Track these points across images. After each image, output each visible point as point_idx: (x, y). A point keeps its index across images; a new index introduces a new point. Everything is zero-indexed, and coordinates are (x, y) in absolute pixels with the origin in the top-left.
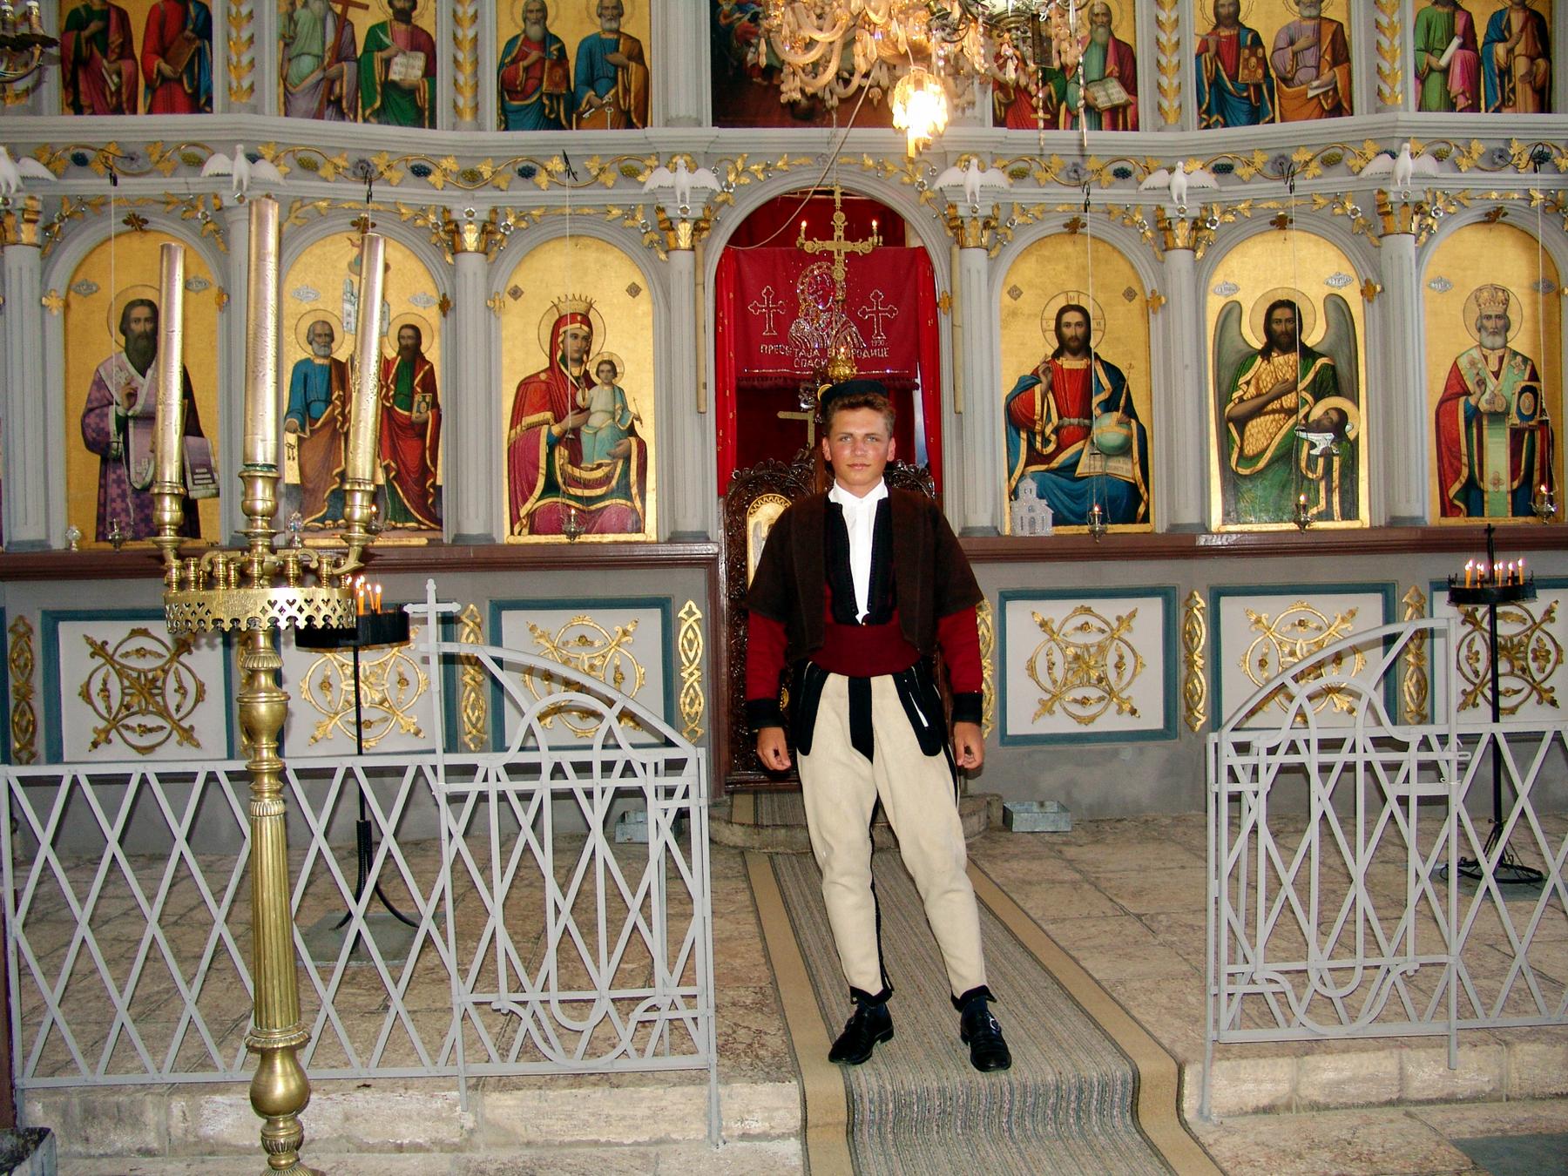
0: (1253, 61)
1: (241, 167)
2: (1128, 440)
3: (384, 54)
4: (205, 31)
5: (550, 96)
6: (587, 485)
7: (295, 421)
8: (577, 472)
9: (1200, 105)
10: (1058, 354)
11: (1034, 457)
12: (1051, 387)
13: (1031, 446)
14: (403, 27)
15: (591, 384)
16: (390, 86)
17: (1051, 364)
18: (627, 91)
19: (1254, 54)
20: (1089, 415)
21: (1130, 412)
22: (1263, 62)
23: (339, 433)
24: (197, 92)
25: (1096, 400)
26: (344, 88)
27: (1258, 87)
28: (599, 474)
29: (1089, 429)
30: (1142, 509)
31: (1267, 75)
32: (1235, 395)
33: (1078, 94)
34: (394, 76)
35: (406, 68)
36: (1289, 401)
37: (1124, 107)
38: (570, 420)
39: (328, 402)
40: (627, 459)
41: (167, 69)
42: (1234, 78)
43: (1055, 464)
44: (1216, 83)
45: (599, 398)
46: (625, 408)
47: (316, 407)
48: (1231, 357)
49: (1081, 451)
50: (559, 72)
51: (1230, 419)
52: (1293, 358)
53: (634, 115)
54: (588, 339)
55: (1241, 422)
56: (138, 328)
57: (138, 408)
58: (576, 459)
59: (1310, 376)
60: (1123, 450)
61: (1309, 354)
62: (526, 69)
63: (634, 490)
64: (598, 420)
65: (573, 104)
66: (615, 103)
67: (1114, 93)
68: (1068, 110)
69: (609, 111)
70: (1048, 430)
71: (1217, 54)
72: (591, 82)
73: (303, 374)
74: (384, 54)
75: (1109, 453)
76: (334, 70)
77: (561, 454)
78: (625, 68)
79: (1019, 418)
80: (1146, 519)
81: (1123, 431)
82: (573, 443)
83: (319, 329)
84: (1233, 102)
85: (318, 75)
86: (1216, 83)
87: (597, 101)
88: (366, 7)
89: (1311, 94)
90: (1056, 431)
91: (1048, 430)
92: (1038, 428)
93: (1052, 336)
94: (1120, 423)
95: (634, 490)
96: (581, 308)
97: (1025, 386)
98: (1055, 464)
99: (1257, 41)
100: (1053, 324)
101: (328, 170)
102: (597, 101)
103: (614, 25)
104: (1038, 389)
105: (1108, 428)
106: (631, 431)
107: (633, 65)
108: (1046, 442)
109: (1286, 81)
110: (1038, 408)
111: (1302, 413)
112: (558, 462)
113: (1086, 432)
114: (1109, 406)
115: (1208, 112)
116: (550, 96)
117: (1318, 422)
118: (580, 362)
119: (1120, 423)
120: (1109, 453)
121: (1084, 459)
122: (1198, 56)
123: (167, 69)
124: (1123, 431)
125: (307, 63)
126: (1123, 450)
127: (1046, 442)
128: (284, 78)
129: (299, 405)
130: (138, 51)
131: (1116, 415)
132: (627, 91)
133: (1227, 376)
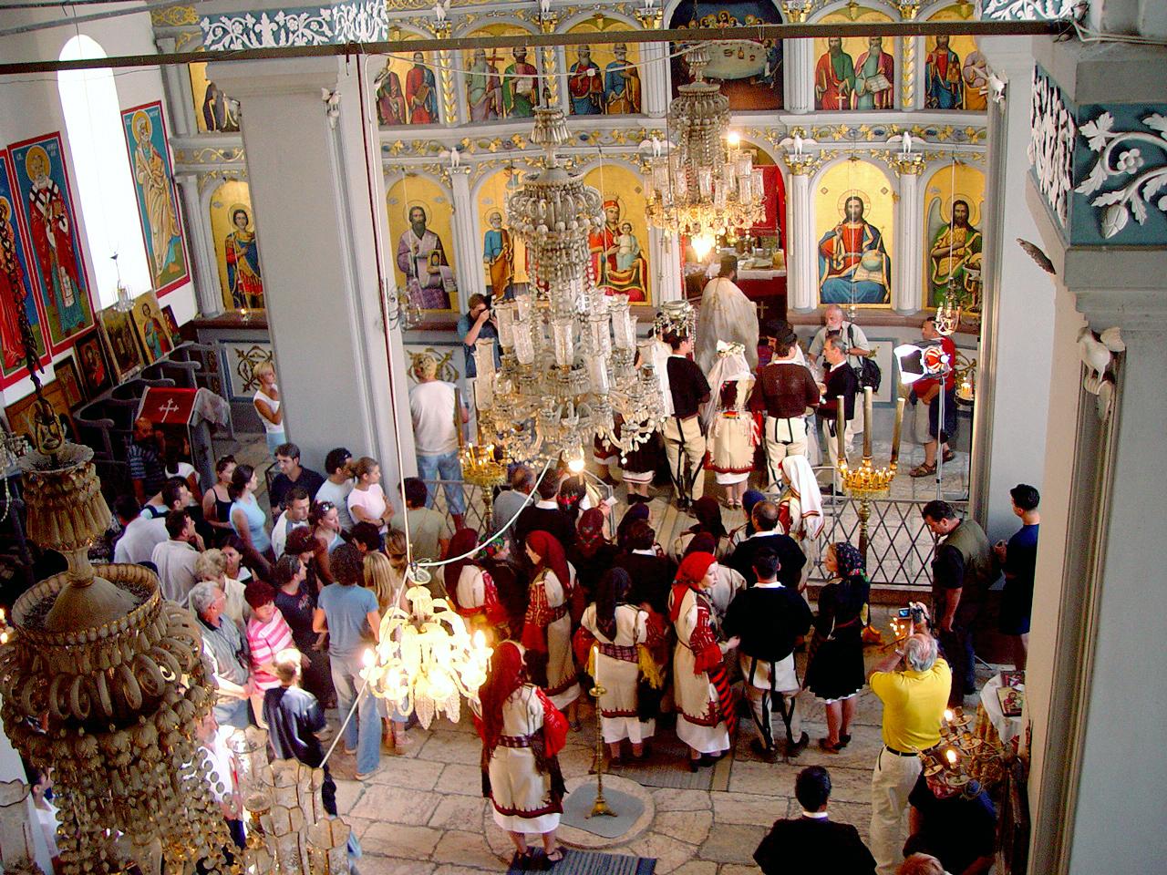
0: (954, 70)
1: (455, 156)
2: (881, 263)
3: (514, 81)
4: (433, 84)
5: (594, 94)
6: (619, 280)
7: (488, 259)
8: (616, 274)
9: (927, 90)
10: (845, 222)
11: (832, 271)
12: (842, 238)
13: (831, 266)
14: (521, 65)
15: (620, 234)
16: (517, 95)
17: (842, 227)
18: (630, 91)
19: (954, 67)
20: (861, 251)
21: (882, 250)
22: (959, 72)
23: (507, 261)
24: (431, 111)
25: (865, 244)
26: (496, 101)
27: (956, 85)
28: (626, 275)
29: (861, 258)
30: (886, 297)
31: (960, 79)
32: (937, 244)
33: (860, 84)
34: (519, 91)
35: (524, 86)
36: (961, 251)
37: (887, 90)
38: (612, 250)
39: (502, 248)
40: (638, 268)
41: (417, 100)
42: (944, 79)
43: (843, 275)
44: (935, 80)
45: (624, 241)
46: (636, 245)
47: (496, 254)
48: (935, 226)
49: (856, 269)
50: (598, 81)
51: (933, 256)
52: (964, 230)
53: (634, 107)
54: (618, 213)
55: (938, 258)
56: (417, 219)
57: (420, 254)
58: (614, 268)
59: (971, 241)
60: (879, 268)
61: (971, 230)
62: (582, 80)
63: (642, 283)
64: (623, 251)
65: (605, 99)
66: (625, 97)
67: (883, 83)
68: (856, 94)
69: (622, 102)
70: (840, 258)
71: (937, 63)
72: (613, 88)
73: (489, 238)
74: (514, 81)
75: (871, 270)
76: (491, 94)
77: (608, 265)
78: (629, 79)
79: (825, 252)
80: (888, 302)
81: (878, 259)
82: (612, 258)
83: (495, 216)
84: (943, 90)
85: (484, 97)
86: (935, 80)
87: (616, 97)
88: (503, 59)
89: (981, 93)
90: (844, 258)
91: (840, 258)
92: (835, 257)
93: (843, 212)
94: (876, 255)
95: (642, 283)
96: (614, 198)
97: (829, 237)
98: (843, 275)
99: (957, 61)
100: (843, 207)
101: (493, 147)
102: (616, 97)
103: (623, 58)
104: (835, 239)
105: (871, 258)
106: (639, 256)
107: (633, 78)
108: (838, 264)
109: (970, 84)
110: (835, 248)
111: (967, 258)
112: (607, 272)
113: (859, 260)
114: (872, 247)
115: (930, 95)
116: (594, 94)
117: (973, 264)
118: (615, 223)
119: (876, 255)
120: (871, 270)
121: (858, 272)
122: (927, 63)
123: (417, 100)
124: (878, 259)
125: (479, 92)
126: (879, 268)
127: (838, 264)
128: (469, 102)
129: (489, 251)
130: (404, 93)
131: (876, 251)
132: (630, 91)
133: (933, 233)
